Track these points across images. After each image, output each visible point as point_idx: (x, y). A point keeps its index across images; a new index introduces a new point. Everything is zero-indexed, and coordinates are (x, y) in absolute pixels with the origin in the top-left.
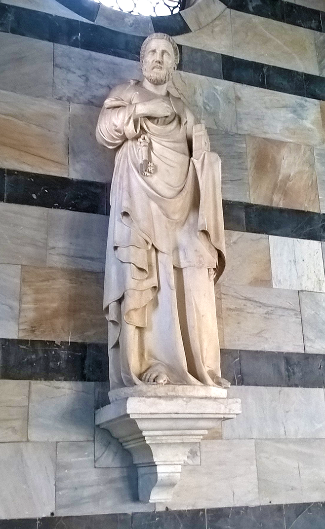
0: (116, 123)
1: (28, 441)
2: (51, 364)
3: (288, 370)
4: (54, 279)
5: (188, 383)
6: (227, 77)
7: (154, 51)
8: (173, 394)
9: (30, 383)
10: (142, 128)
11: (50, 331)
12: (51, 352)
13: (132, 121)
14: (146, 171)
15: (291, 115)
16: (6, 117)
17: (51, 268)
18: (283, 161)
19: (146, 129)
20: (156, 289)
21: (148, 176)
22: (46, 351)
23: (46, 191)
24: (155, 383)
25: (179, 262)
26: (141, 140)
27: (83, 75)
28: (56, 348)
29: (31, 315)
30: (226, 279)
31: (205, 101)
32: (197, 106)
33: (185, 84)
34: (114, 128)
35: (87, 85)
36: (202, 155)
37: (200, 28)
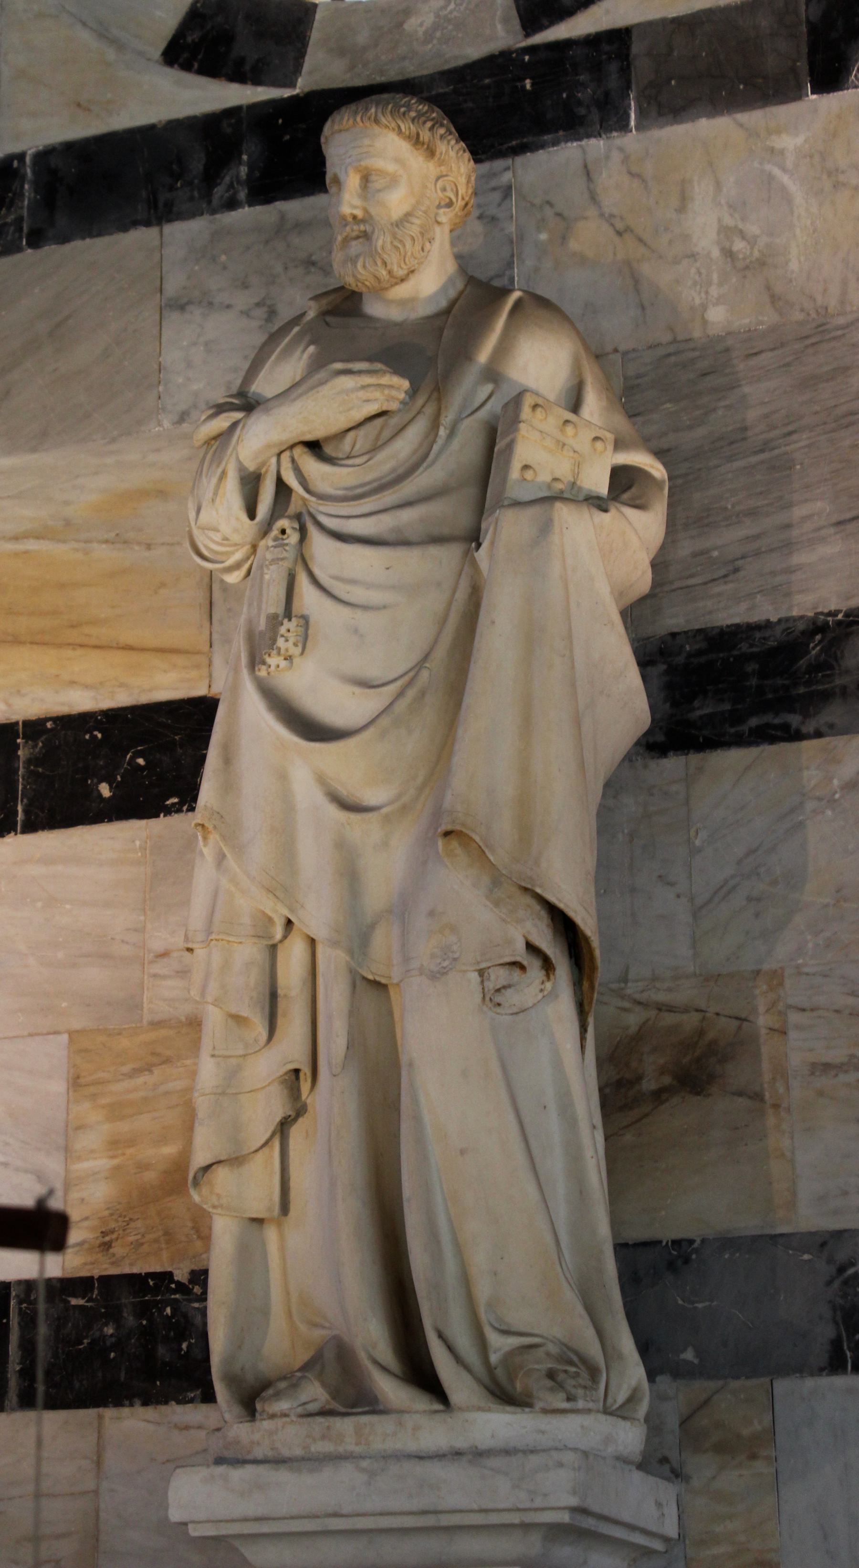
2: (162, 1351)
4: (168, 1061)
9: (100, 1417)
11: (156, 1241)
12: (161, 1310)
16: (20, 547)
22: (143, 1310)
23: (141, 761)
27: (258, 305)
28: (177, 1296)
30: (810, 945)
32: (693, 256)
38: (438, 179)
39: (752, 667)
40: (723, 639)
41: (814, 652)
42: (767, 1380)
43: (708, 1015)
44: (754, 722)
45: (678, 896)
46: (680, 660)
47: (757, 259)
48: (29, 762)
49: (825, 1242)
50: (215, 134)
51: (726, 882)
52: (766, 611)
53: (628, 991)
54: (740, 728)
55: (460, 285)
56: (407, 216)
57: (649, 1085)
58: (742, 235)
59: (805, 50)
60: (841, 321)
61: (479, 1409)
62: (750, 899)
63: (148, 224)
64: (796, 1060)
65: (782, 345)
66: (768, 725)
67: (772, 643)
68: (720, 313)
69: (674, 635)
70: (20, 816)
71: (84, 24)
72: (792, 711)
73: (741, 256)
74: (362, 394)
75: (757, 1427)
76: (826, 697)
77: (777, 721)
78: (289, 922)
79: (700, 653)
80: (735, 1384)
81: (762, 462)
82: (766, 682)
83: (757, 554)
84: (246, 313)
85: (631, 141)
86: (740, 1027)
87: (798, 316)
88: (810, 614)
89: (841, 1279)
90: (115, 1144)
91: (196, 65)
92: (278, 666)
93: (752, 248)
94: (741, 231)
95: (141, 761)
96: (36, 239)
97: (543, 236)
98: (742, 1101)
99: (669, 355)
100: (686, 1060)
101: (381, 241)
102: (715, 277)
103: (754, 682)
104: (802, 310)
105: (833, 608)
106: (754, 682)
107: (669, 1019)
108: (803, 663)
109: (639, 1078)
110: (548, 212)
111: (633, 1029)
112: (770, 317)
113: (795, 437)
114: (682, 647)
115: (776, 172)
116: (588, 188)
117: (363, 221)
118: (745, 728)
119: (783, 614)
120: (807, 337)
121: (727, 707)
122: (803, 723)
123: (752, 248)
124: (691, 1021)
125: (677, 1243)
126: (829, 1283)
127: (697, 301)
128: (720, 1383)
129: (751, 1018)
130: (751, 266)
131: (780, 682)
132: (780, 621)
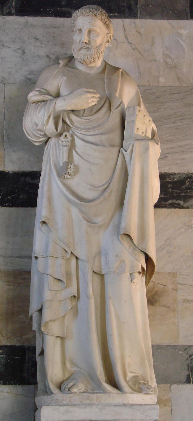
0: (37, 122)
5: (104, 391)
7: (80, 30)
8: (88, 402)
13: (51, 120)
14: (66, 174)
19: (70, 125)
21: (68, 179)
24: (69, 392)
26: (62, 138)
27: (19, 49)
30: (184, 267)
31: (166, 53)
32: (155, 61)
33: (141, 35)
34: (35, 127)
35: (23, 59)
36: (131, 146)
38: (107, 34)
39: (170, 186)
41: (187, 184)
42: (169, 385)
43: (155, 283)
44: (170, 202)
47: (174, 66)
54: (166, 203)
56: (101, 45)
59: (189, 5)
61: (131, 393)
62: (168, 252)
67: (175, 180)
72: (181, 200)
73: (169, 64)
74: (92, 100)
77: (177, 202)
81: (174, 126)
82: (174, 191)
83: (172, 153)
84: (15, 51)
85: (138, 21)
86: (164, 288)
87: (185, 85)
88: (187, 173)
89: (190, 359)
92: (67, 177)
93: (172, 62)
94: (169, 56)
98: (164, 308)
99: (148, 89)
102: (162, 68)
103: (170, 190)
104: (186, 84)
106: (170, 190)
112: (177, 84)
113: (183, 121)
116: (124, 33)
118: (168, 203)
119: (179, 172)
120: (187, 92)
122: (184, 204)
123: (172, 62)
126: (187, 360)
127: (156, 75)
129: (167, 285)
131: (177, 191)
132: (178, 173)
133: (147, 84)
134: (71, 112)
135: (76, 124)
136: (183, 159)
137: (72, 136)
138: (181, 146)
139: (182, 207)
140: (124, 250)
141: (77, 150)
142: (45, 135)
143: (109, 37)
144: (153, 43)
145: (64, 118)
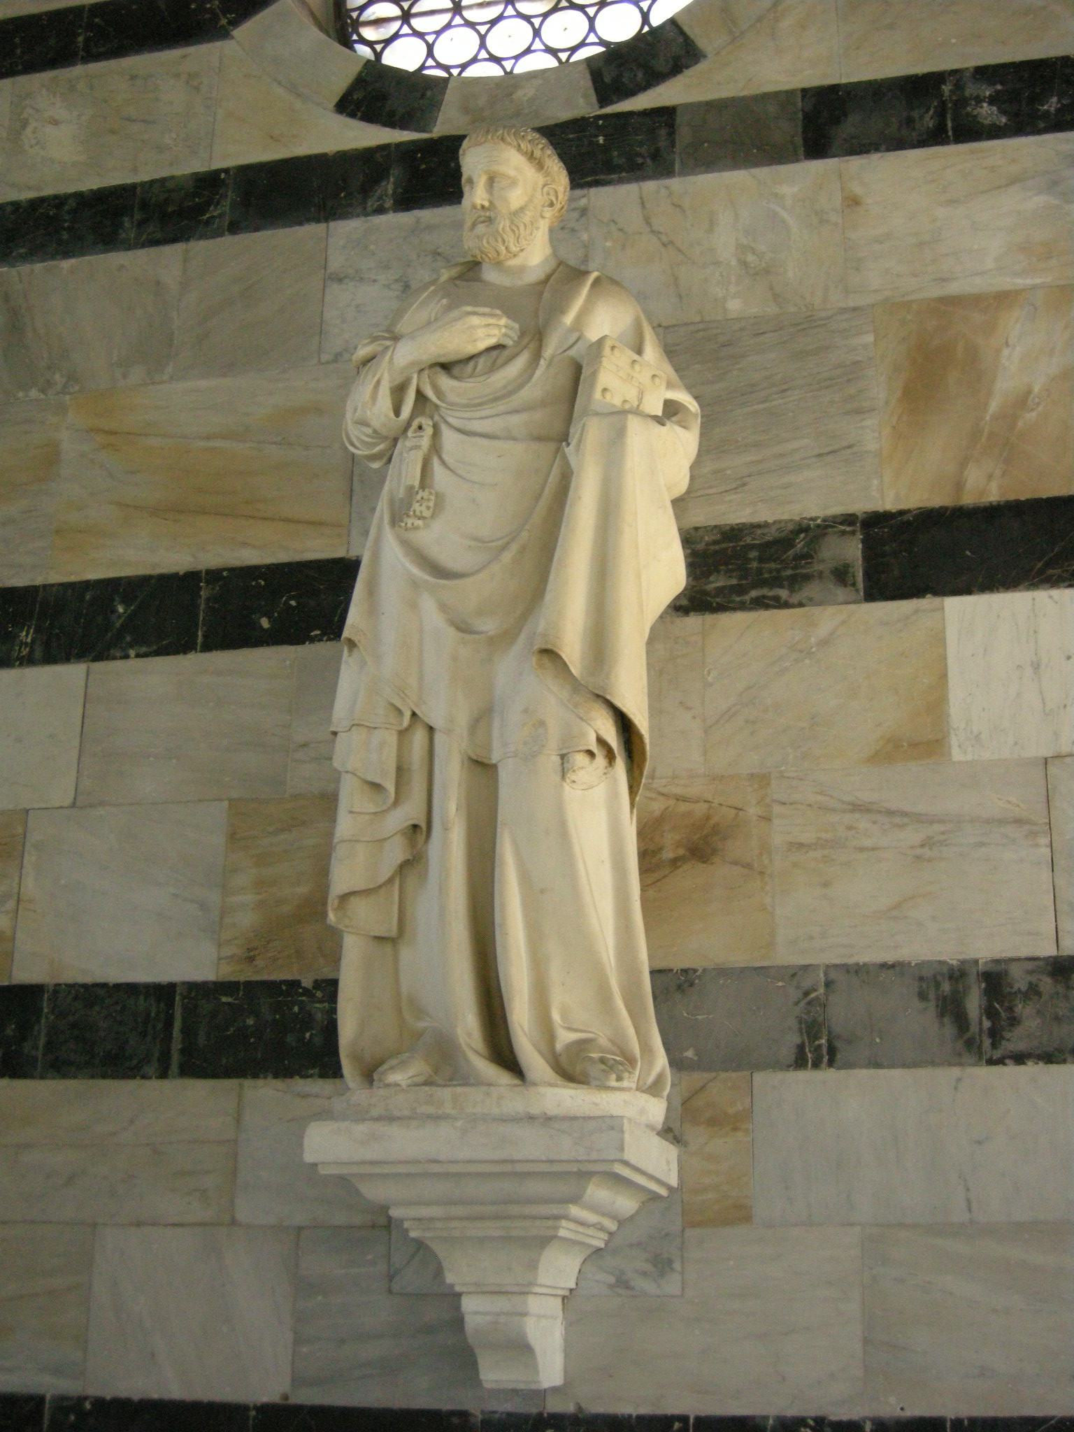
1: (234, 1222)
3: (990, 1013)
4: (304, 823)
5: (479, 1082)
6: (817, 147)
8: (430, 1110)
10: (420, 395)
14: (408, 516)
15: (1038, 201)
16: (211, 444)
17: (295, 797)
18: (1006, 352)
19: (438, 402)
20: (418, 832)
25: (488, 747)
27: (396, 281)
29: (246, 920)
31: (745, 242)
37: (734, 39)
39: (753, 554)
40: (733, 533)
44: (754, 593)
45: (694, 717)
46: (701, 547)
48: (208, 600)
49: (795, 973)
50: (370, 165)
51: (730, 709)
52: (765, 514)
53: (654, 786)
55: (553, 264)
56: (522, 209)
57: (668, 854)
58: (753, 251)
59: (800, 130)
60: (823, 314)
61: (551, 1085)
62: (747, 722)
63: (318, 221)
64: (778, 840)
65: (781, 329)
66: (764, 597)
67: (768, 538)
68: (737, 305)
69: (696, 529)
70: (200, 640)
71: (279, 83)
72: (782, 587)
75: (739, 1107)
76: (807, 578)
77: (770, 594)
78: (414, 714)
79: (715, 542)
80: (724, 1075)
84: (388, 286)
85: (675, 183)
86: (737, 815)
87: (792, 309)
88: (797, 518)
90: (260, 884)
91: (359, 114)
95: (293, 603)
96: (234, 228)
97: (608, 244)
100: (695, 837)
101: (503, 224)
103: (755, 565)
105: (814, 515)
106: (755, 565)
107: (683, 807)
108: (791, 553)
109: (661, 849)
110: (613, 228)
111: (657, 813)
112: (772, 309)
113: (789, 393)
114: (702, 538)
115: (778, 209)
117: (488, 209)
118: (747, 598)
120: (799, 324)
121: (734, 582)
124: (700, 809)
125: (685, 971)
126: (797, 1004)
127: (720, 295)
128: (714, 1074)
130: (759, 272)
132: (775, 522)
133: (698, 319)
134: (438, 369)
135: (452, 397)
136: (787, 486)
137: (436, 427)
138: (781, 455)
139: (786, 605)
140: (550, 700)
141: (444, 456)
142: (385, 438)
143: (552, 193)
144: (712, 224)
145: (421, 385)
